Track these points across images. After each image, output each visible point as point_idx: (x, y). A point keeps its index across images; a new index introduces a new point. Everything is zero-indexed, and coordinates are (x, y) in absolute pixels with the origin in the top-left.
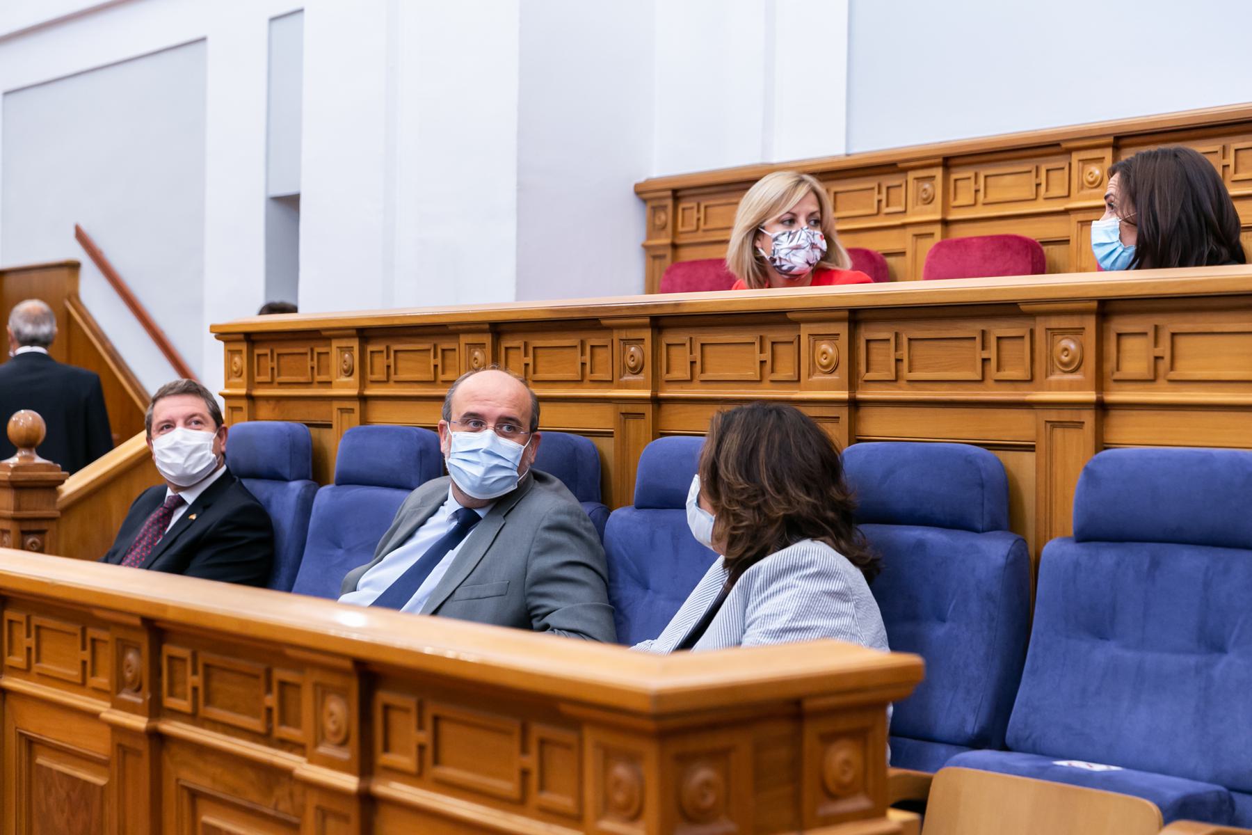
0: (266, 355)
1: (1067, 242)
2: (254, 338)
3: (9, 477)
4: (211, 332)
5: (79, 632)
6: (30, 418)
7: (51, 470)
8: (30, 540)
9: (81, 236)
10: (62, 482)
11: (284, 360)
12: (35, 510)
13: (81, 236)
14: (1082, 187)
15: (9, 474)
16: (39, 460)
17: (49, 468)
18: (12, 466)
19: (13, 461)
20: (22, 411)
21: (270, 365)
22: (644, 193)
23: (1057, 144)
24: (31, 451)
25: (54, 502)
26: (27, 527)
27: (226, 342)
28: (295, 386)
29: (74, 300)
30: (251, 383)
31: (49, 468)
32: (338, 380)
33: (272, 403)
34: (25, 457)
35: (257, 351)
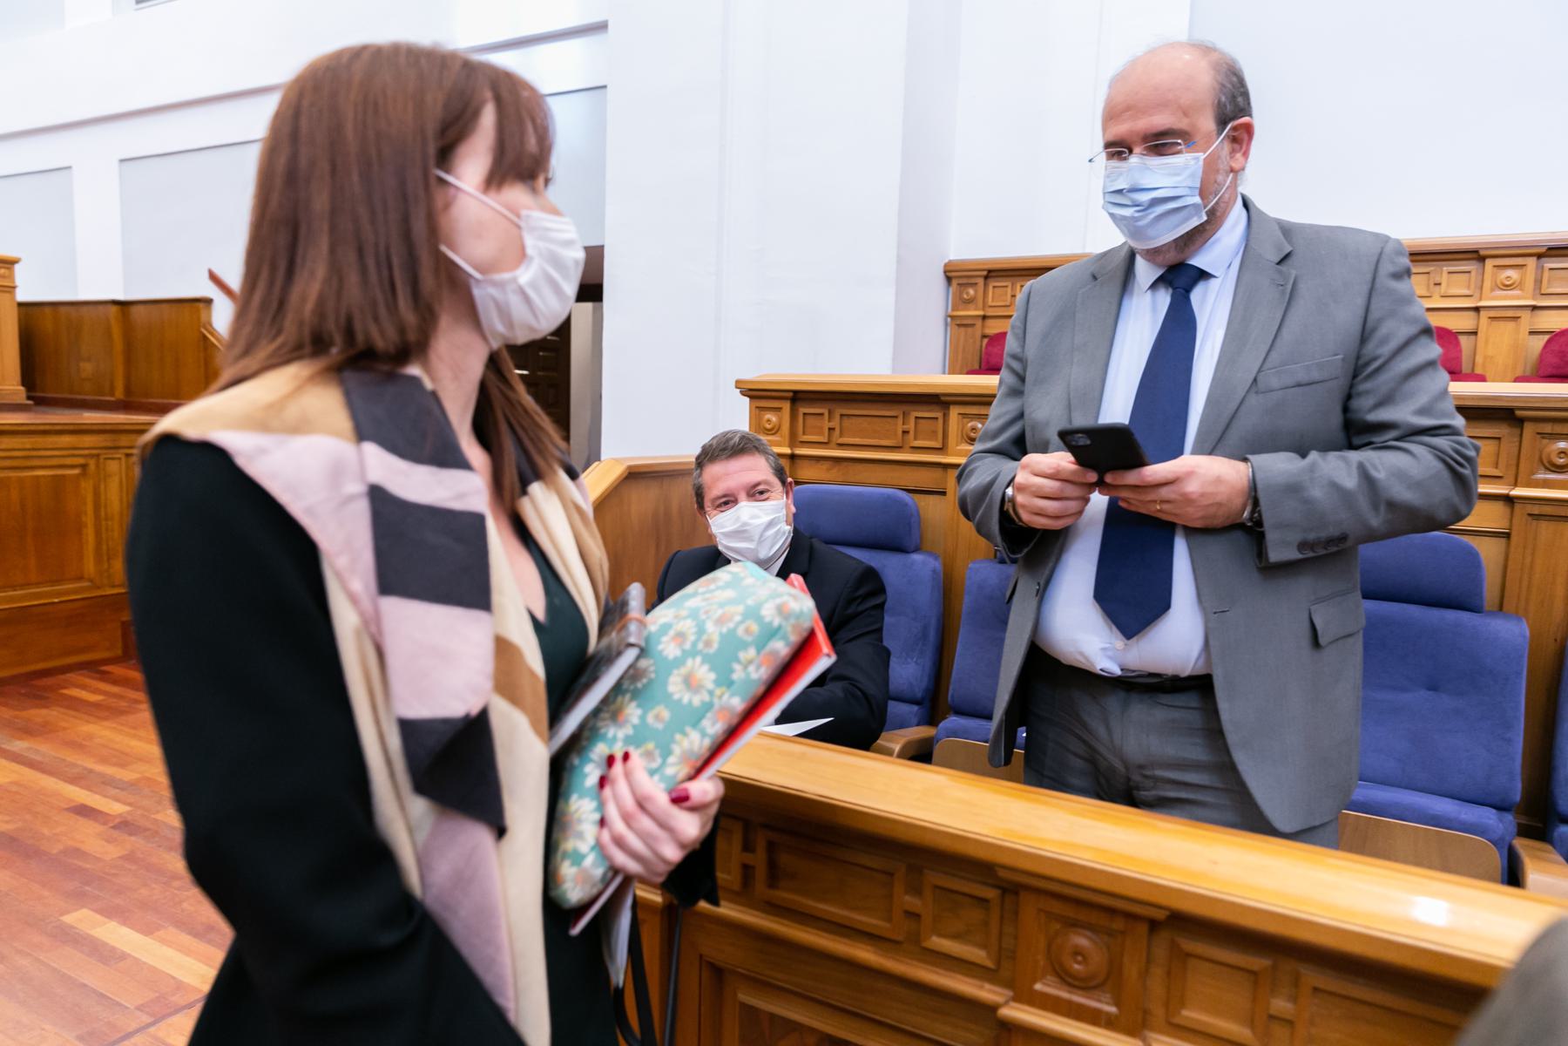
0: (822, 414)
1: (1531, 333)
2: (799, 395)
4: (737, 387)
9: (214, 277)
11: (847, 422)
13: (214, 277)
14: (1492, 290)
21: (827, 425)
22: (956, 275)
23: (1476, 252)
27: (751, 397)
28: (872, 449)
29: (209, 327)
30: (793, 441)
32: (959, 448)
33: (826, 465)
35: (803, 410)
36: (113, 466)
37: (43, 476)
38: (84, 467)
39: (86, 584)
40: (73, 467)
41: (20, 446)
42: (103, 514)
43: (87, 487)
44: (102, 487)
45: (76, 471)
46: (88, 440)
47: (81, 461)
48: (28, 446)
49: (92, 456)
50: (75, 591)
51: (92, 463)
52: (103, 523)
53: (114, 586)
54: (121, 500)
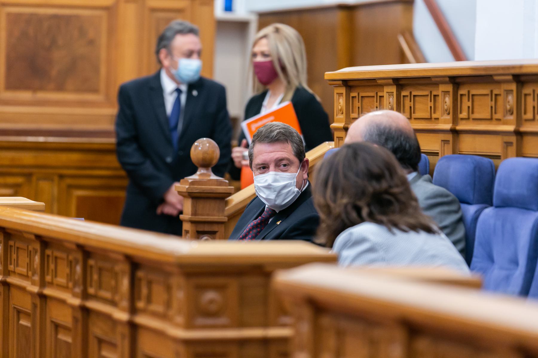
3: (187, 189)
5: (26, 248)
6: (208, 145)
7: (220, 185)
10: (230, 194)
11: (366, 100)
12: (208, 215)
15: (187, 187)
16: (214, 177)
17: (220, 183)
18: (190, 181)
19: (195, 177)
20: (205, 139)
24: (207, 170)
25: (223, 211)
26: (201, 228)
31: (220, 183)
34: (201, 175)
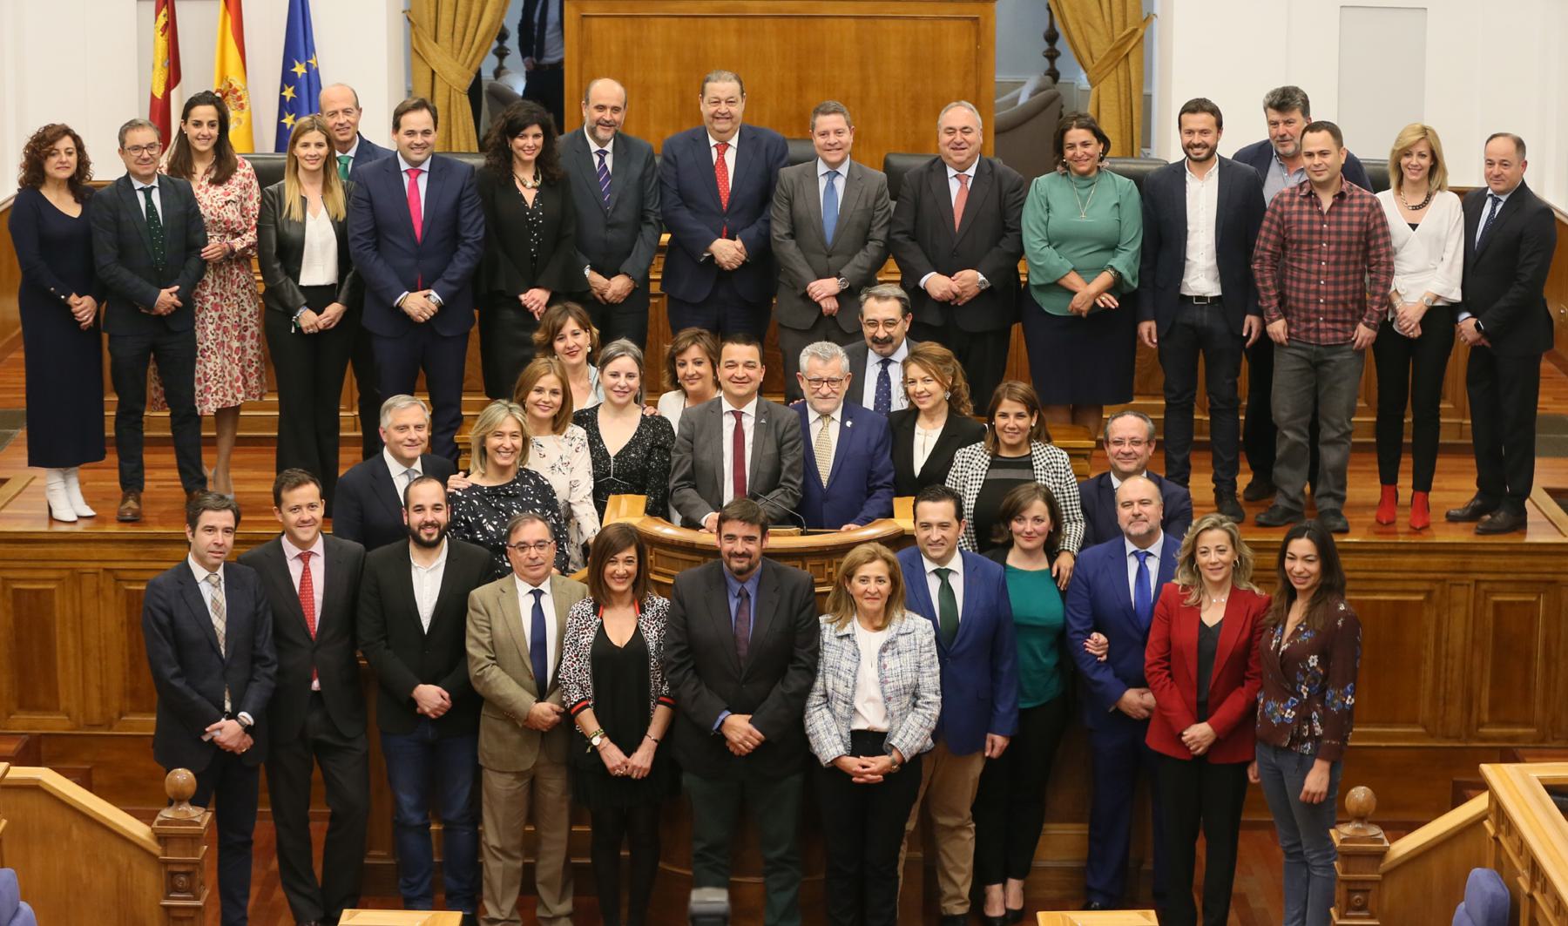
8: (1357, 897)
12: (1361, 873)
25: (1378, 867)
36: (1460, 595)
37: (1385, 601)
38: (1429, 593)
39: (1420, 730)
40: (1417, 592)
41: (1363, 568)
42: (1443, 652)
43: (1429, 615)
44: (1446, 617)
45: (1421, 598)
46: (1435, 561)
47: (1426, 586)
48: (1370, 568)
49: (1437, 581)
50: (1407, 737)
51: (1437, 587)
52: (1443, 660)
53: (1448, 737)
54: (1465, 633)
